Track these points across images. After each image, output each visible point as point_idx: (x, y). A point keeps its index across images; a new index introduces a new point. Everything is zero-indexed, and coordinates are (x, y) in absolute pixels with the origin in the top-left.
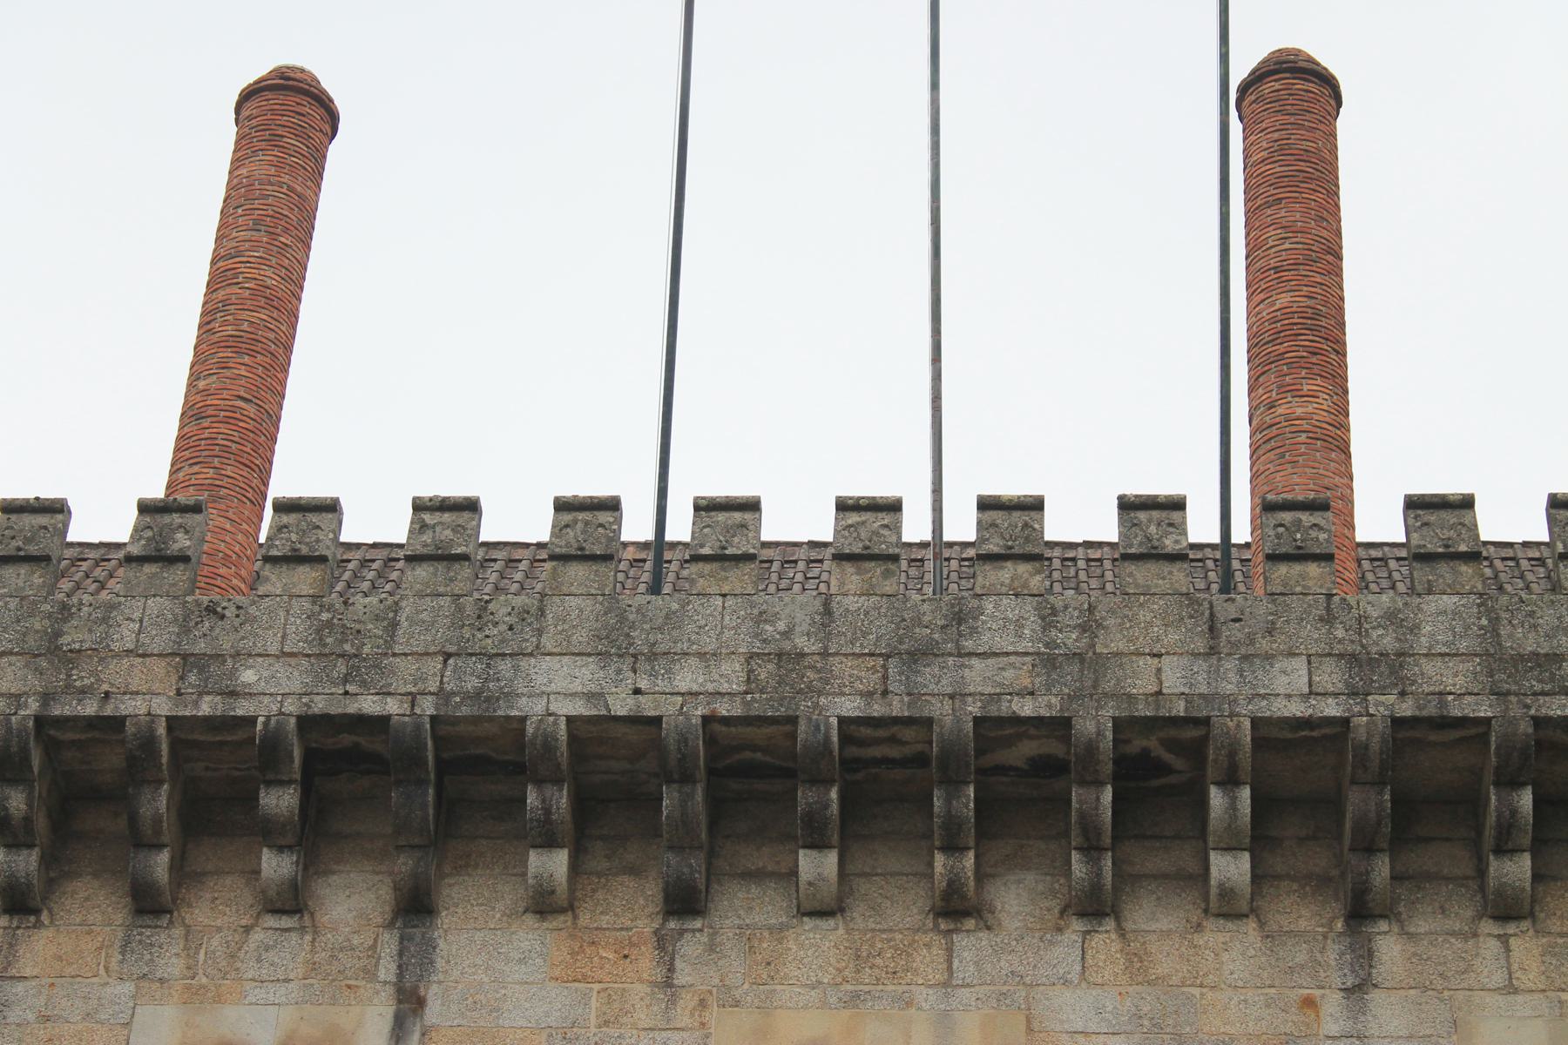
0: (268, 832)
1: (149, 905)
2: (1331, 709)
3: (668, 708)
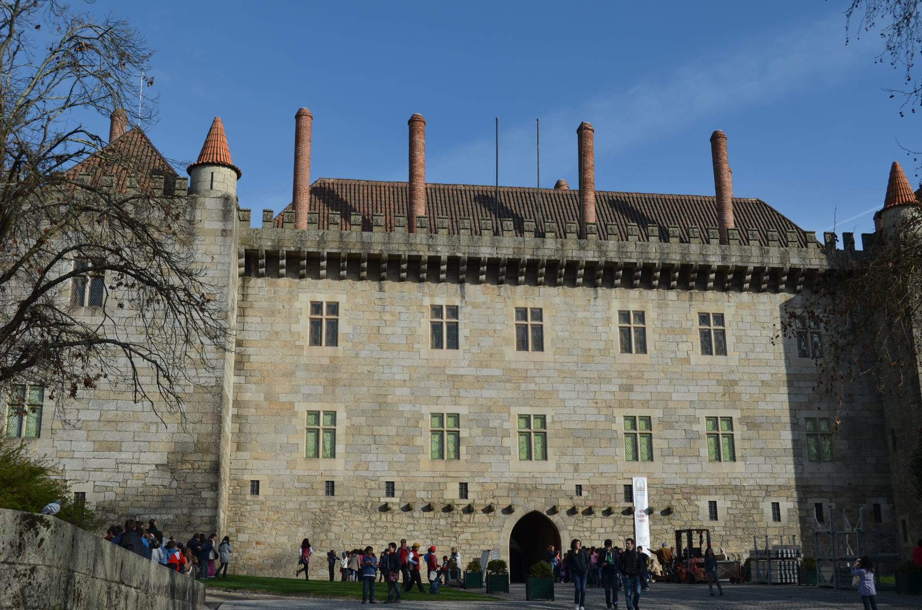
2: (596, 260)
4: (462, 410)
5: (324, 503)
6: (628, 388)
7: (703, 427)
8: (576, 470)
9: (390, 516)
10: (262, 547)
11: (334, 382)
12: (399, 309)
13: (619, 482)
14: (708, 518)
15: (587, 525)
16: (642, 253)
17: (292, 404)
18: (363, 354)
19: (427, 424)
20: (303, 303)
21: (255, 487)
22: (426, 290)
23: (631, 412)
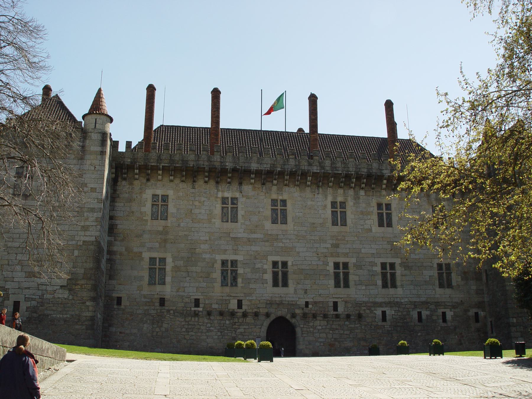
0: (229, 178)
1: (217, 183)
2: (318, 171)
3: (264, 169)
4: (239, 258)
5: (159, 311)
6: (336, 246)
7: (378, 269)
8: (306, 292)
9: (196, 319)
10: (123, 335)
11: (165, 241)
12: (203, 199)
13: (330, 300)
14: (381, 320)
15: (311, 324)
16: (345, 167)
17: (141, 253)
18: (182, 225)
19: (218, 266)
20: (148, 194)
21: (119, 300)
22: (220, 188)
23: (337, 260)
